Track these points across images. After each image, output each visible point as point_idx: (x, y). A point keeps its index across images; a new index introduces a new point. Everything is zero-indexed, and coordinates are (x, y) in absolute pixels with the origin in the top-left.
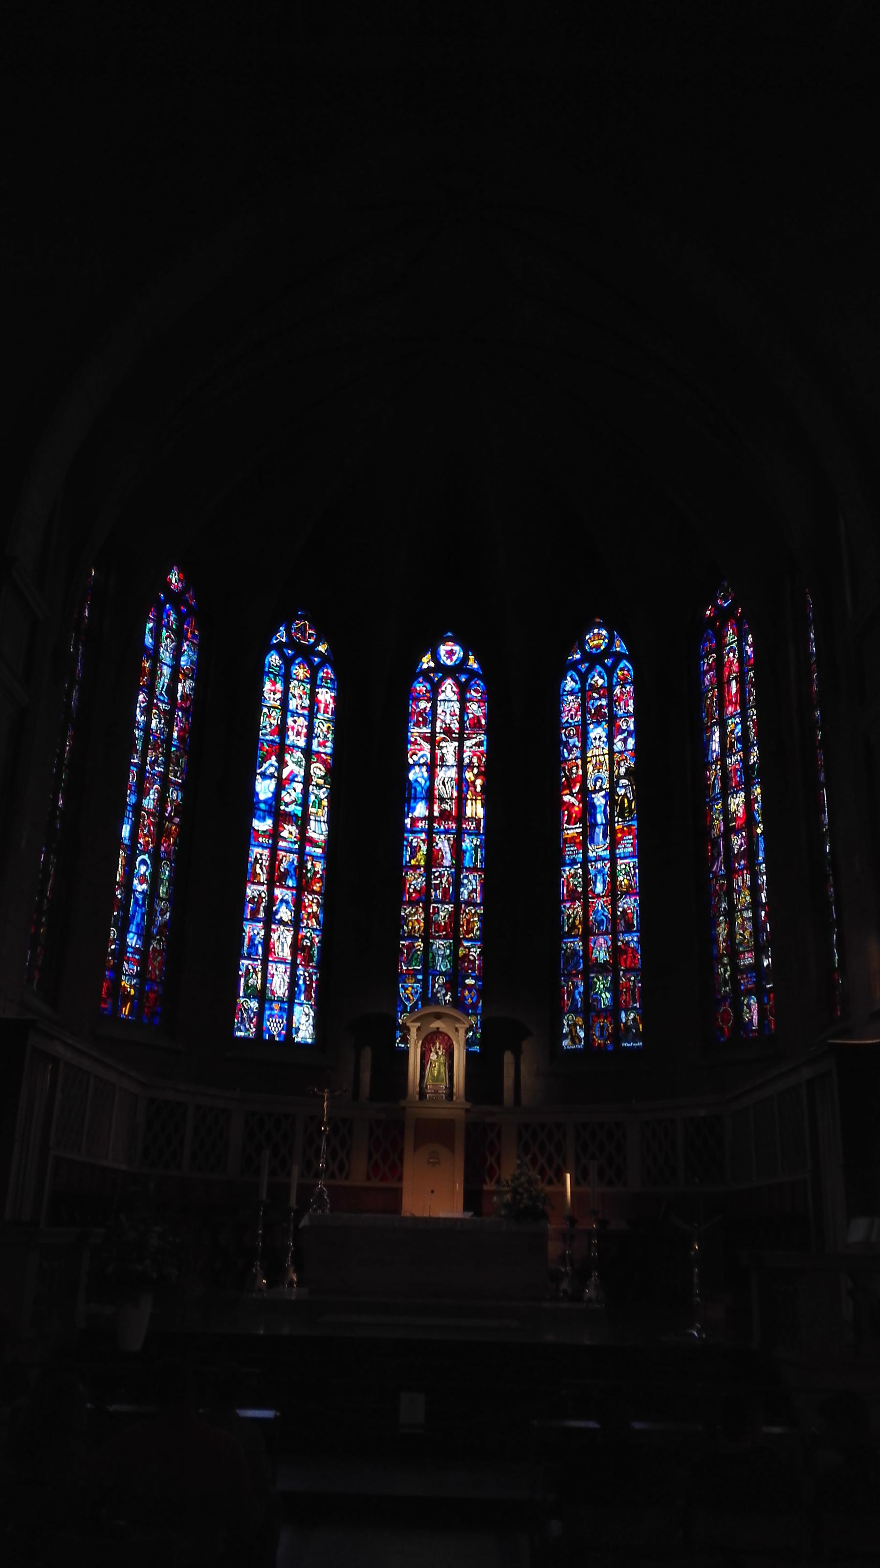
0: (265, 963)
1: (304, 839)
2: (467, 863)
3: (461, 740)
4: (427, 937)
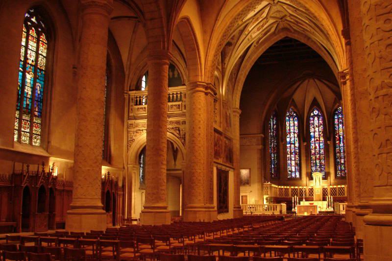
0: (291, 166)
1: (295, 147)
2: (321, 148)
3: (319, 127)
4: (315, 160)
